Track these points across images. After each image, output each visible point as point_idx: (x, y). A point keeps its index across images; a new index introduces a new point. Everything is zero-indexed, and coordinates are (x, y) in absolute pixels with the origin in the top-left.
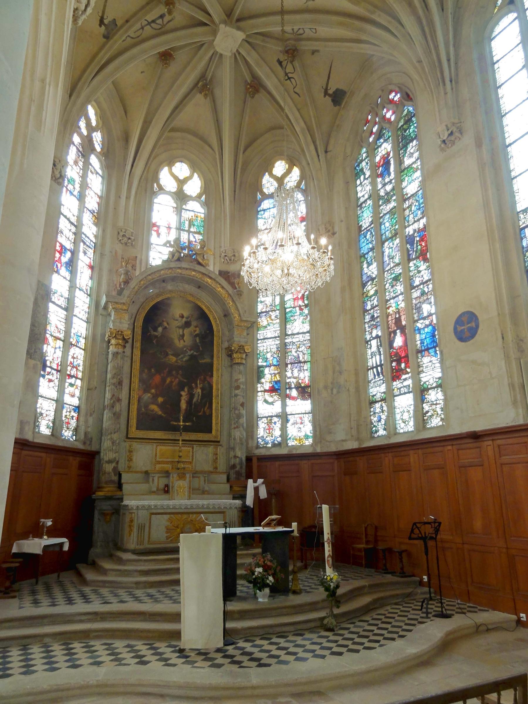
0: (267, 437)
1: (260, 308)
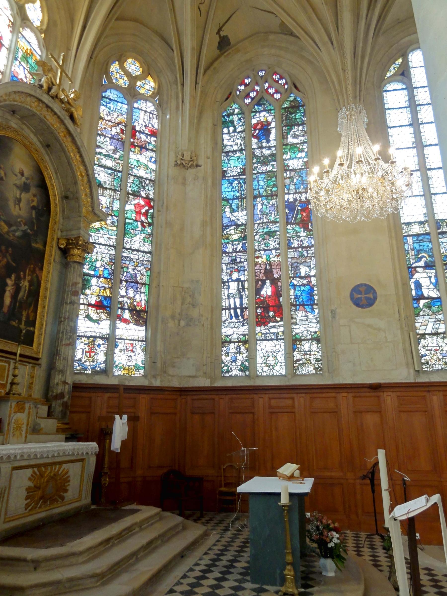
0: (85, 361)
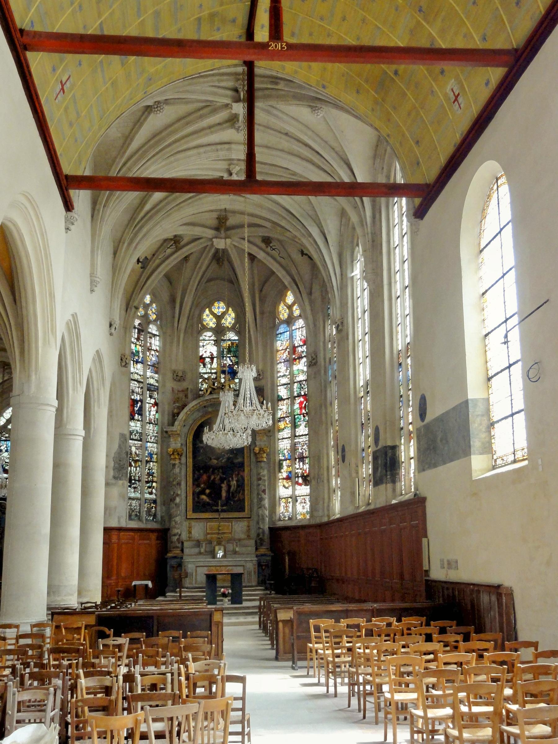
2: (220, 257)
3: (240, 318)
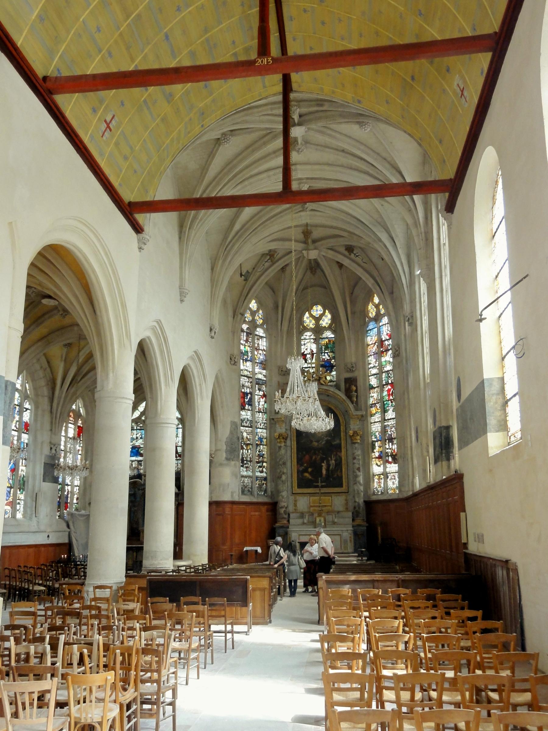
1: (371, 401)
2: (314, 267)
3: (335, 319)
